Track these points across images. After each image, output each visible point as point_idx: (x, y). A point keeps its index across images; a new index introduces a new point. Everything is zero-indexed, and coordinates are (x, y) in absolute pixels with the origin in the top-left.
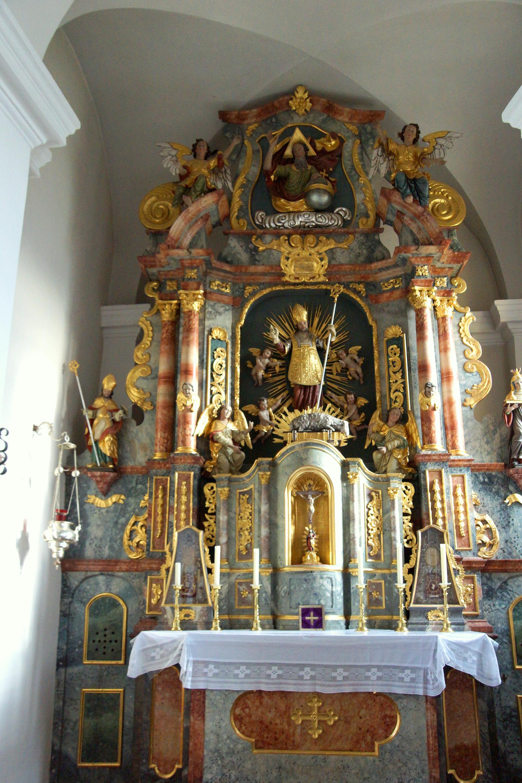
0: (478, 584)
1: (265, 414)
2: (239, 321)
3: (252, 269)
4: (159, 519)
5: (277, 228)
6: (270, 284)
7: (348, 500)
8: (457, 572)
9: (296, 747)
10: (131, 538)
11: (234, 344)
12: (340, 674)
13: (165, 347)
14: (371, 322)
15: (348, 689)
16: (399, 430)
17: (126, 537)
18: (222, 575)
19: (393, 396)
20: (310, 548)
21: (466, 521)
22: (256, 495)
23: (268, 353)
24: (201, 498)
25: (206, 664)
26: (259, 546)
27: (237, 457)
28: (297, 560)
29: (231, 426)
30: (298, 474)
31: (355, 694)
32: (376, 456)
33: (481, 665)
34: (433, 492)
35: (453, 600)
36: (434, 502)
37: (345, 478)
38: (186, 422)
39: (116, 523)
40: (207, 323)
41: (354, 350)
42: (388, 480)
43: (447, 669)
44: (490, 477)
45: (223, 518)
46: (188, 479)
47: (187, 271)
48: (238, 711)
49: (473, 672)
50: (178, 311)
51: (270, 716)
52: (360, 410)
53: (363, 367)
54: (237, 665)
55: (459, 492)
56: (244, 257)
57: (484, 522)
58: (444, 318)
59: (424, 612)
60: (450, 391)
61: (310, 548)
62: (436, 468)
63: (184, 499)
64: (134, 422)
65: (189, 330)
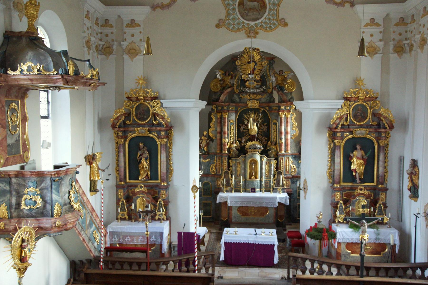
0: (290, 182)
1: (243, 141)
3: (240, 104)
4: (219, 166)
5: (246, 92)
7: (261, 164)
8: (284, 180)
9: (249, 216)
10: (212, 169)
11: (235, 123)
12: (258, 203)
13: (219, 125)
14: (269, 117)
15: (259, 206)
16: (274, 147)
18: (234, 180)
19: (274, 137)
20: (253, 175)
21: (289, 168)
22: (241, 163)
23: (244, 125)
25: (232, 201)
27: (237, 153)
28: (250, 178)
29: (235, 145)
30: (251, 159)
32: (269, 153)
34: (281, 163)
35: (283, 186)
36: (281, 165)
37: (261, 160)
38: (225, 146)
39: (208, 166)
40: (229, 119)
41: (265, 124)
42: (271, 160)
43: (278, 202)
44: (296, 156)
45: (234, 168)
46: (226, 159)
47: (224, 107)
48: (239, 209)
49: (284, 202)
50: (222, 115)
51: (244, 210)
52: (266, 140)
54: (238, 202)
56: (238, 100)
57: (293, 167)
58: (288, 118)
59: (277, 189)
60: (287, 137)
61: (253, 175)
62: (282, 157)
63: (225, 163)
64: (211, 142)
65: (225, 122)
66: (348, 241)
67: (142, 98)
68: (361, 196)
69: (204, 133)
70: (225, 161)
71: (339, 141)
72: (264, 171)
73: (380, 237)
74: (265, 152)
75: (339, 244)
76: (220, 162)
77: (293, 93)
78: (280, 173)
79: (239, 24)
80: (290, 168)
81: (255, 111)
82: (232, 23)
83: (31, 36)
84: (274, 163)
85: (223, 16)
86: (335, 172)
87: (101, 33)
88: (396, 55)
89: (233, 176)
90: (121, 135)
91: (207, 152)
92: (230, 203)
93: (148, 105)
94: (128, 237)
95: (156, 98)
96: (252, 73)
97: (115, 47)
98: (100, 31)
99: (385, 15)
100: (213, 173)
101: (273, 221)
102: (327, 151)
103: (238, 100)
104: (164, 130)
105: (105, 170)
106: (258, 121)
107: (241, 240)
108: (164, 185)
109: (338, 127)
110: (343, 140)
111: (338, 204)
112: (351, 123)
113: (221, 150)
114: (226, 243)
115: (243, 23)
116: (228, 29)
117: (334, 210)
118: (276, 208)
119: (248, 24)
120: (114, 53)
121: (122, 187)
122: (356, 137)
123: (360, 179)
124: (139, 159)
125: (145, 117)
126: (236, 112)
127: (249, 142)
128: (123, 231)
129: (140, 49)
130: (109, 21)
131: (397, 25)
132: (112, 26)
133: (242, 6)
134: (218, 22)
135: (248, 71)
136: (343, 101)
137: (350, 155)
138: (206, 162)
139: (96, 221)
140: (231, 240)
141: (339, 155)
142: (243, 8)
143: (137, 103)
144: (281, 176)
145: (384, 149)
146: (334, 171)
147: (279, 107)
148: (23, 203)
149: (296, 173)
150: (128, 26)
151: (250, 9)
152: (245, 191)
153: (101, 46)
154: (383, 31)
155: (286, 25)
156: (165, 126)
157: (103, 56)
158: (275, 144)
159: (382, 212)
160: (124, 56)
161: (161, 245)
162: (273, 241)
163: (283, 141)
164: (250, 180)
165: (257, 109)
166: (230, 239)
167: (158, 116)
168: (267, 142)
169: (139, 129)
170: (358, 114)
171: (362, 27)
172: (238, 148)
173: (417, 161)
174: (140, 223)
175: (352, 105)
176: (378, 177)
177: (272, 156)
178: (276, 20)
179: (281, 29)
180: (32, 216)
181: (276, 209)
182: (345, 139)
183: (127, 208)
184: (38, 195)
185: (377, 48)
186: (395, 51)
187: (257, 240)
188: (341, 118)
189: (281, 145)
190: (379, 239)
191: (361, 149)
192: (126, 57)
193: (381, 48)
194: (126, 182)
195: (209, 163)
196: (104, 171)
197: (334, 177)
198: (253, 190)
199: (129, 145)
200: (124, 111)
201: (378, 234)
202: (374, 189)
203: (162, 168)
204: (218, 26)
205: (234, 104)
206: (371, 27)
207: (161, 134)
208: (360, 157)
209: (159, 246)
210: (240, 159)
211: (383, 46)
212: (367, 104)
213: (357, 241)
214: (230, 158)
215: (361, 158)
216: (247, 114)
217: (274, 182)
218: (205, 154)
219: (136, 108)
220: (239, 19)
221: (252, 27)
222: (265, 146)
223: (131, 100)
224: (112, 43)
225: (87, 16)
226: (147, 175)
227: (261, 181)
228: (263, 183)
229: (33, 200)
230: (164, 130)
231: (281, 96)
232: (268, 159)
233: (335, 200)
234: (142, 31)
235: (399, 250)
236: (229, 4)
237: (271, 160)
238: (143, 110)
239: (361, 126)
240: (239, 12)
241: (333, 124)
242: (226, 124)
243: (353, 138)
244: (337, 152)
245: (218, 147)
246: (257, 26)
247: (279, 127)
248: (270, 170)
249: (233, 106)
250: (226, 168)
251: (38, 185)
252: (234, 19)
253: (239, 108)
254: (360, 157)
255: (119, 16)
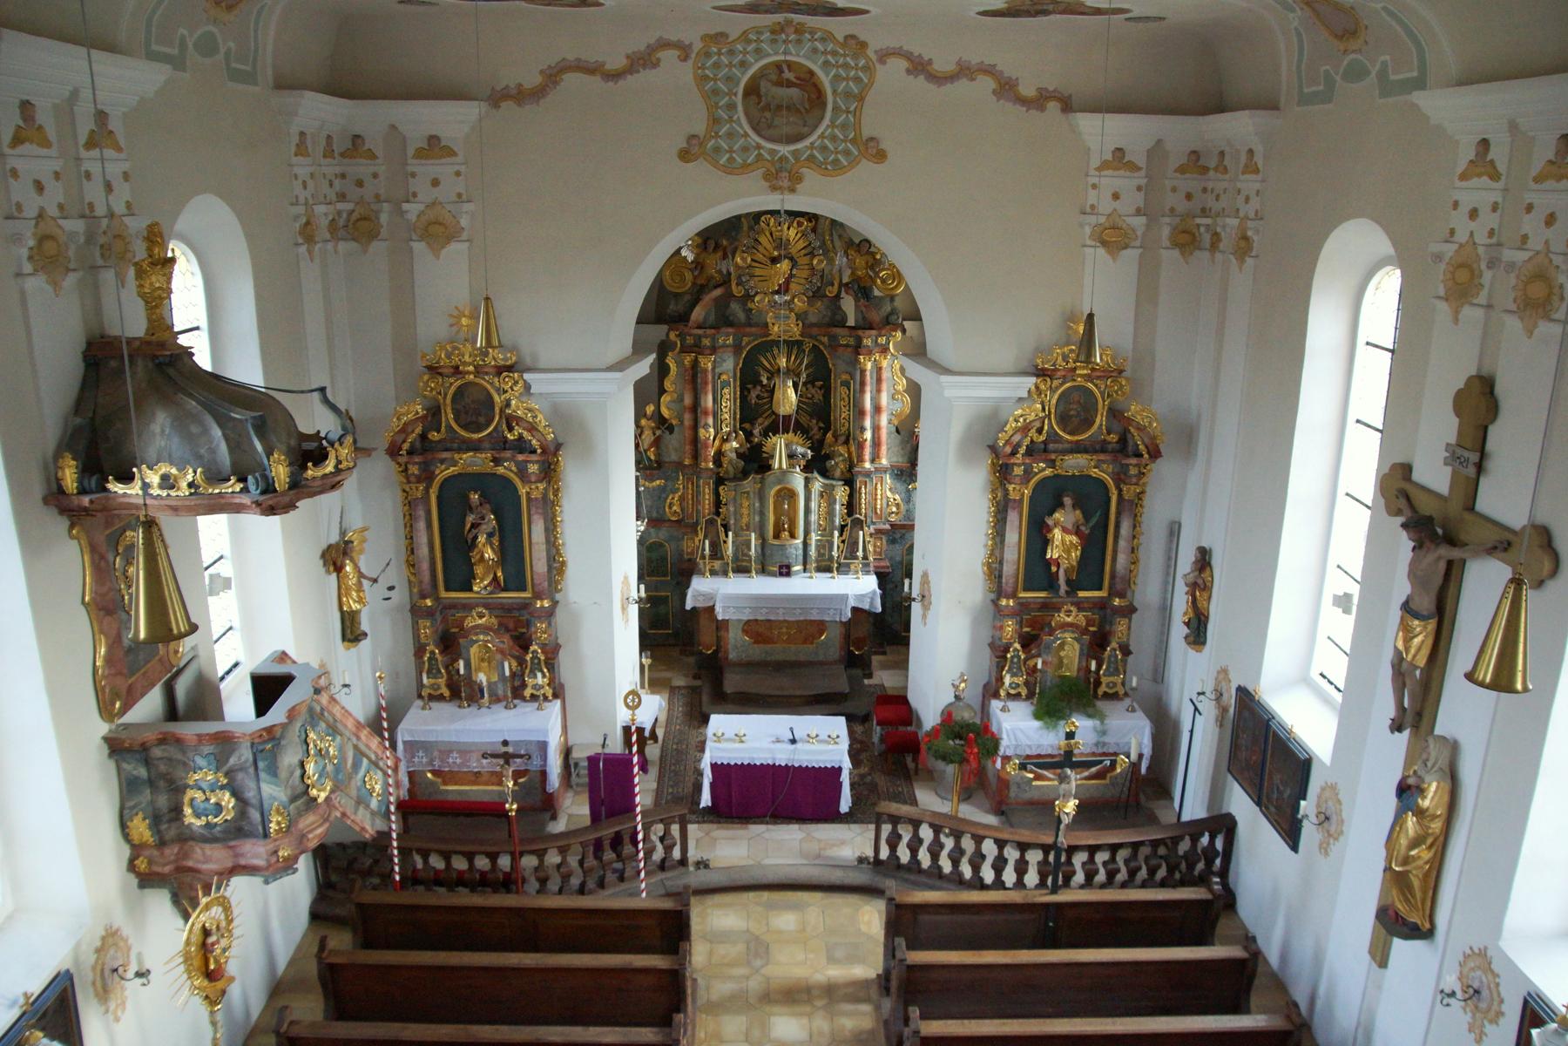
0: (884, 541)
1: (756, 432)
2: (738, 365)
3: (748, 330)
6: (762, 337)
10: (670, 508)
11: (735, 381)
13: (688, 387)
15: (802, 618)
16: (842, 449)
17: (667, 510)
18: (733, 542)
19: (843, 421)
21: (881, 504)
22: (752, 495)
23: (759, 388)
24: (717, 494)
26: (755, 531)
28: (777, 536)
29: (735, 444)
31: (806, 620)
33: (872, 603)
34: (860, 494)
35: (865, 557)
36: (860, 500)
37: (806, 486)
38: (706, 446)
39: (660, 498)
40: (717, 370)
42: (833, 486)
44: (902, 471)
47: (703, 340)
49: (866, 607)
52: (820, 428)
53: (824, 396)
55: (879, 485)
56: (741, 316)
58: (880, 368)
59: (848, 565)
60: (879, 420)
61: (784, 530)
63: (707, 497)
65: (706, 383)
66: (1029, 752)
67: (471, 368)
68: (1068, 631)
69: (647, 408)
70: (707, 490)
71: (1018, 487)
72: (813, 518)
73: (1106, 739)
74: (817, 464)
75: (1006, 759)
76: (693, 490)
77: (897, 299)
78: (859, 524)
79: (745, 149)
80: (885, 501)
81: (792, 345)
82: (727, 148)
83: (156, 357)
84: (841, 493)
85: (700, 128)
86: (1005, 568)
87: (343, 176)
88: (1176, 253)
89: (730, 534)
90: (416, 472)
91: (657, 462)
92: (724, 611)
93: (488, 387)
94: (455, 755)
95: (510, 369)
96: (784, 289)
97: (384, 218)
98: (338, 170)
99: (1154, 143)
100: (674, 519)
101: (838, 654)
102: (986, 510)
103: (741, 316)
104: (537, 462)
105: (379, 580)
106: (798, 375)
107: (753, 758)
108: (542, 607)
109: (1017, 452)
110: (1029, 481)
111: (1009, 651)
112: (1053, 437)
113: (696, 456)
114: (715, 767)
115: (759, 147)
116: (716, 165)
117: (998, 663)
118: (845, 623)
119: (772, 152)
120: (384, 232)
121: (429, 613)
122: (1064, 473)
123: (1069, 582)
124: (470, 536)
125: (482, 420)
126: (737, 348)
127: (774, 435)
128: (440, 739)
129: (458, 222)
130: (363, 140)
131: (1182, 170)
132: (372, 156)
133: (754, 97)
134: (685, 145)
135: (773, 285)
136: (1033, 379)
137: (1045, 522)
138: (654, 489)
139: (370, 748)
140: (729, 758)
141: (1017, 523)
142: (759, 103)
143: (456, 381)
144: (861, 533)
145: (1132, 507)
146: (1001, 563)
147: (859, 340)
148: (188, 811)
149: (900, 516)
150: (420, 154)
151: (779, 107)
152: (763, 571)
153: (345, 215)
154: (1146, 185)
155: (881, 156)
156: (539, 451)
157: (353, 245)
158: (847, 442)
159: (1117, 669)
160: (412, 244)
161: (544, 774)
162: (837, 758)
163: (868, 435)
164: (776, 542)
165: (797, 341)
166: (724, 754)
167: (517, 424)
168: (825, 435)
169: (465, 456)
170: (1072, 413)
171: (1092, 172)
172: (742, 451)
173: (1210, 550)
174: (484, 710)
175: (1057, 388)
176: (1113, 576)
177: (838, 473)
178: (853, 141)
179: (866, 167)
180: (213, 840)
181: (847, 625)
182: (1036, 478)
183: (447, 668)
184: (222, 788)
185: (1129, 232)
186: (1176, 244)
187: (796, 757)
188: (1025, 429)
189: (861, 446)
190: (1104, 744)
191: (1074, 507)
192: (419, 247)
193: (1139, 233)
194: (437, 599)
195: (663, 489)
196: (375, 581)
197: (1000, 576)
198: (785, 571)
199: (439, 498)
200: (419, 408)
201: (1104, 733)
202: (1102, 605)
203: (538, 562)
204: (685, 155)
205: (730, 330)
206: (1116, 173)
207: (530, 471)
208: (1070, 527)
209: (538, 774)
210: (749, 484)
211: (1143, 228)
212: (1096, 386)
213: (1050, 752)
214: (720, 481)
215: (1074, 531)
216: (768, 355)
217: (841, 545)
218: (650, 468)
219: (455, 394)
220: (746, 135)
221: (783, 159)
222: (817, 446)
223: (440, 374)
224: (374, 207)
225: (301, 149)
226: (495, 578)
227: (806, 544)
228: (813, 552)
229: (212, 801)
230: (537, 462)
231: (864, 309)
232: (827, 485)
233: (1000, 639)
234: (463, 169)
235: (1149, 768)
236: (715, 92)
237: (833, 486)
238: (473, 402)
239: (1078, 448)
240: (746, 114)
241: (1005, 445)
242: (710, 387)
243: (1057, 476)
244: (1012, 517)
245: (688, 447)
246: (797, 160)
247: (858, 395)
248: (830, 513)
249: (728, 335)
250: (709, 509)
251: (219, 762)
252: (730, 135)
253: (746, 339)
254: (1070, 527)
255: (393, 127)
